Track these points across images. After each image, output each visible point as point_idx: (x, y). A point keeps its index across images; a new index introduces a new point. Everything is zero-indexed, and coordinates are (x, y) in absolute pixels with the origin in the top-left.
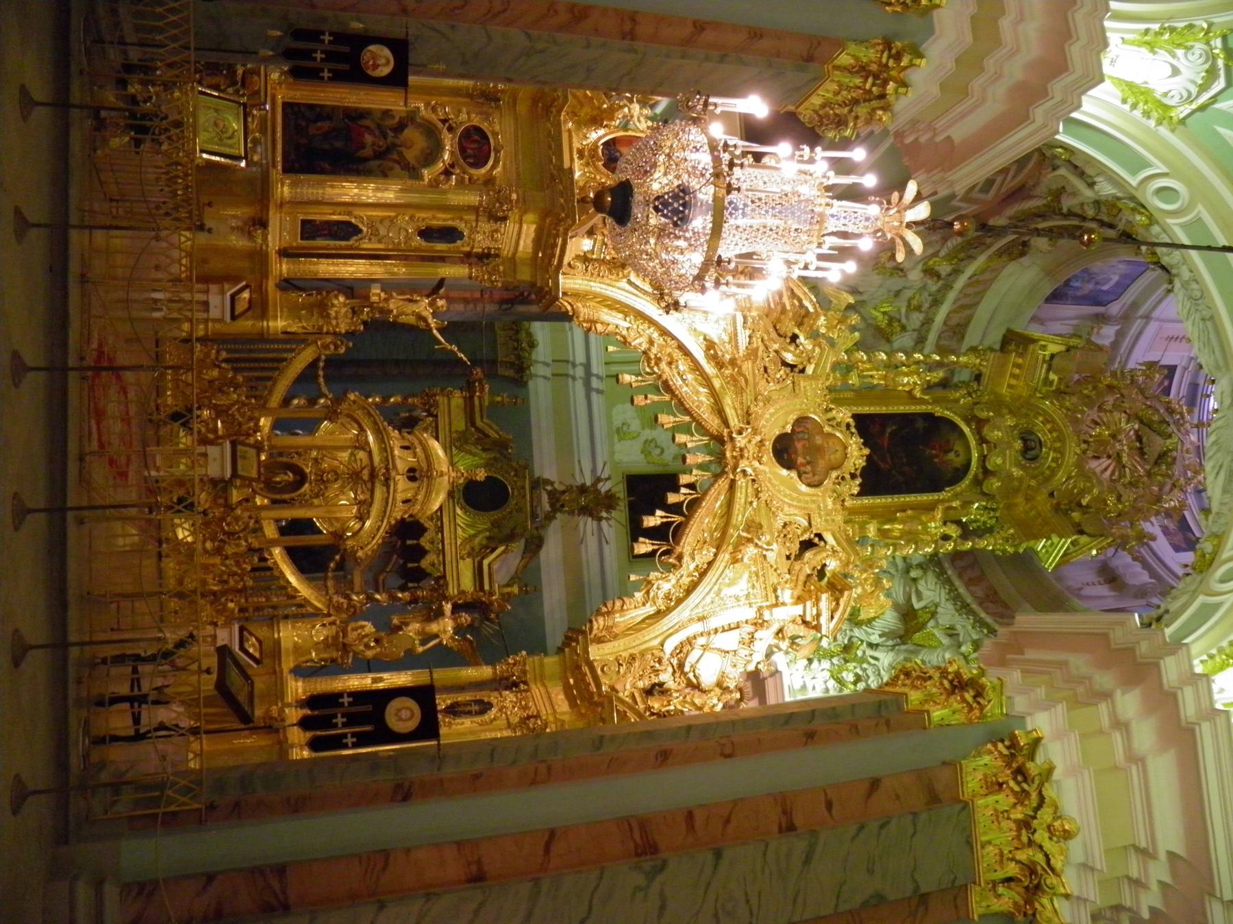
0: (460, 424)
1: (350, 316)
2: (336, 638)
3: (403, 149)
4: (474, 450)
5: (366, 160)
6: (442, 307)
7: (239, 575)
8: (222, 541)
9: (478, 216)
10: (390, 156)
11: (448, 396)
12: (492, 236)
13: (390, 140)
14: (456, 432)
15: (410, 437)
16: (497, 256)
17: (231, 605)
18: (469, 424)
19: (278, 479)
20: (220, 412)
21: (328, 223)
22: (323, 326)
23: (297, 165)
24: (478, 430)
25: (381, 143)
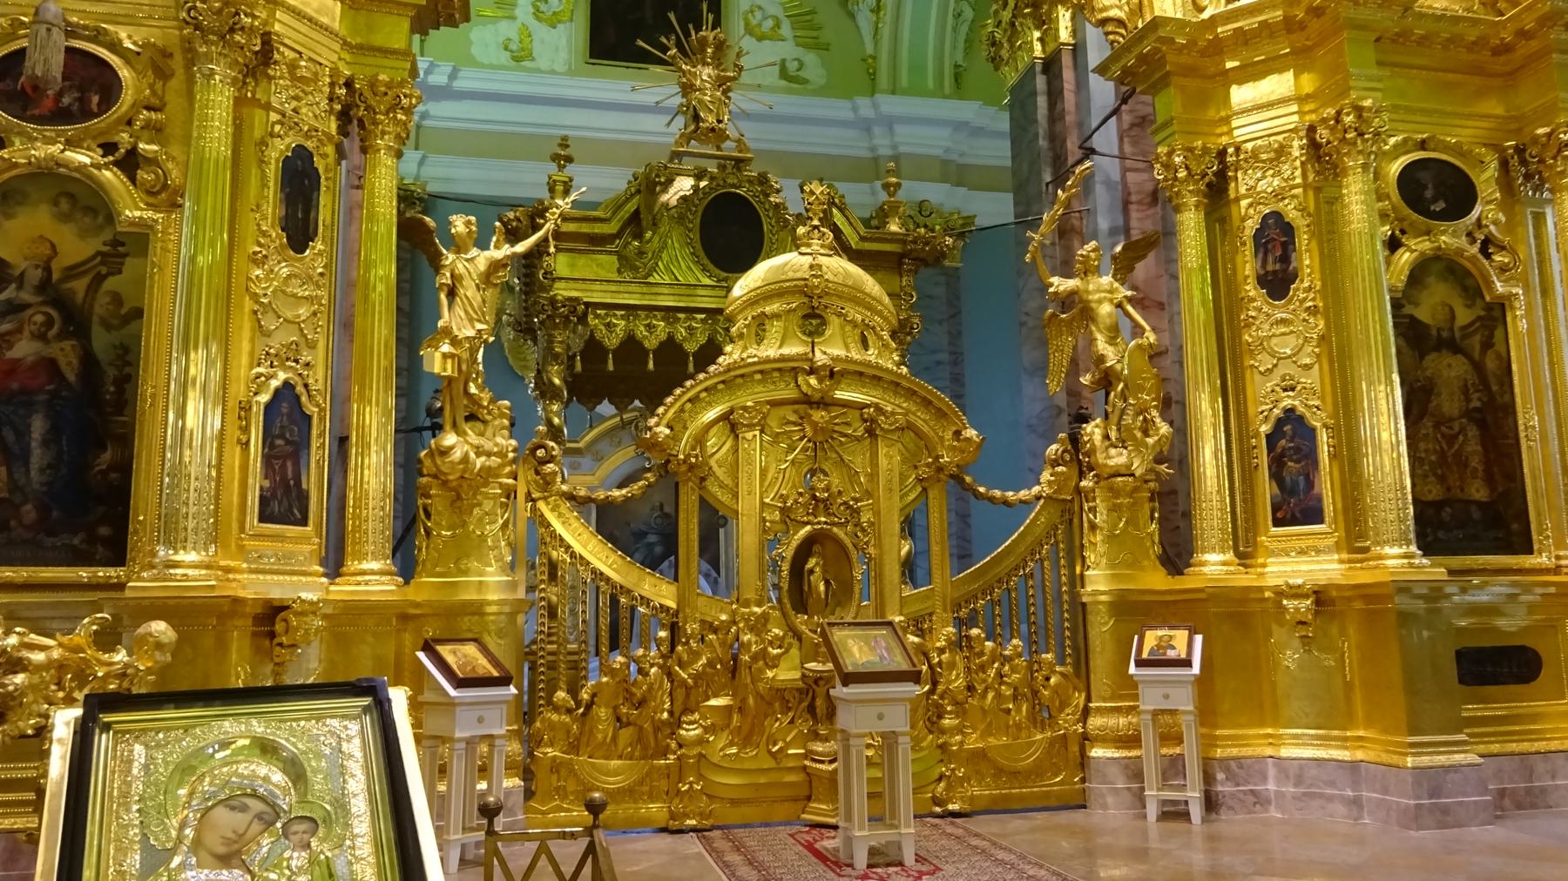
0: (604, 264)
1: (479, 425)
2: (1114, 492)
3: (57, 267)
4: (656, 243)
5: (88, 361)
6: (468, 224)
7: (1003, 665)
8: (942, 697)
9: (255, 102)
10: (80, 296)
11: (554, 280)
12: (302, 79)
13: (26, 296)
14: (619, 271)
15: (741, 323)
16: (349, 84)
17: (1053, 680)
18: (609, 248)
19: (822, 587)
20: (687, 700)
21: (268, 460)
22: (500, 484)
23: (104, 531)
24: (618, 235)
25: (39, 318)
